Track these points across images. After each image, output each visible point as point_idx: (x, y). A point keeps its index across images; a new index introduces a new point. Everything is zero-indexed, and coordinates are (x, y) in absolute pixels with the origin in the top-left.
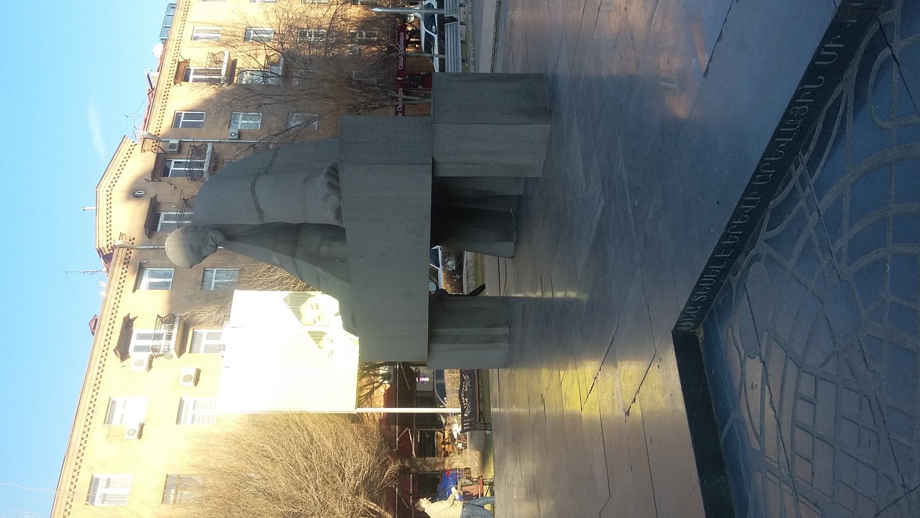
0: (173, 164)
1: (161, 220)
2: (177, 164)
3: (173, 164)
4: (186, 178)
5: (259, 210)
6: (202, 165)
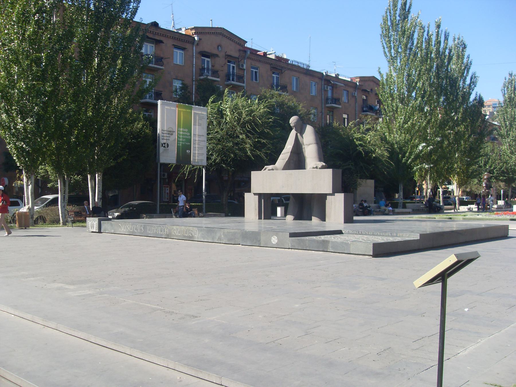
0: (234, 65)
1: (206, 59)
2: (233, 67)
3: (234, 65)
4: (226, 72)
5: (309, 145)
6: (233, 80)
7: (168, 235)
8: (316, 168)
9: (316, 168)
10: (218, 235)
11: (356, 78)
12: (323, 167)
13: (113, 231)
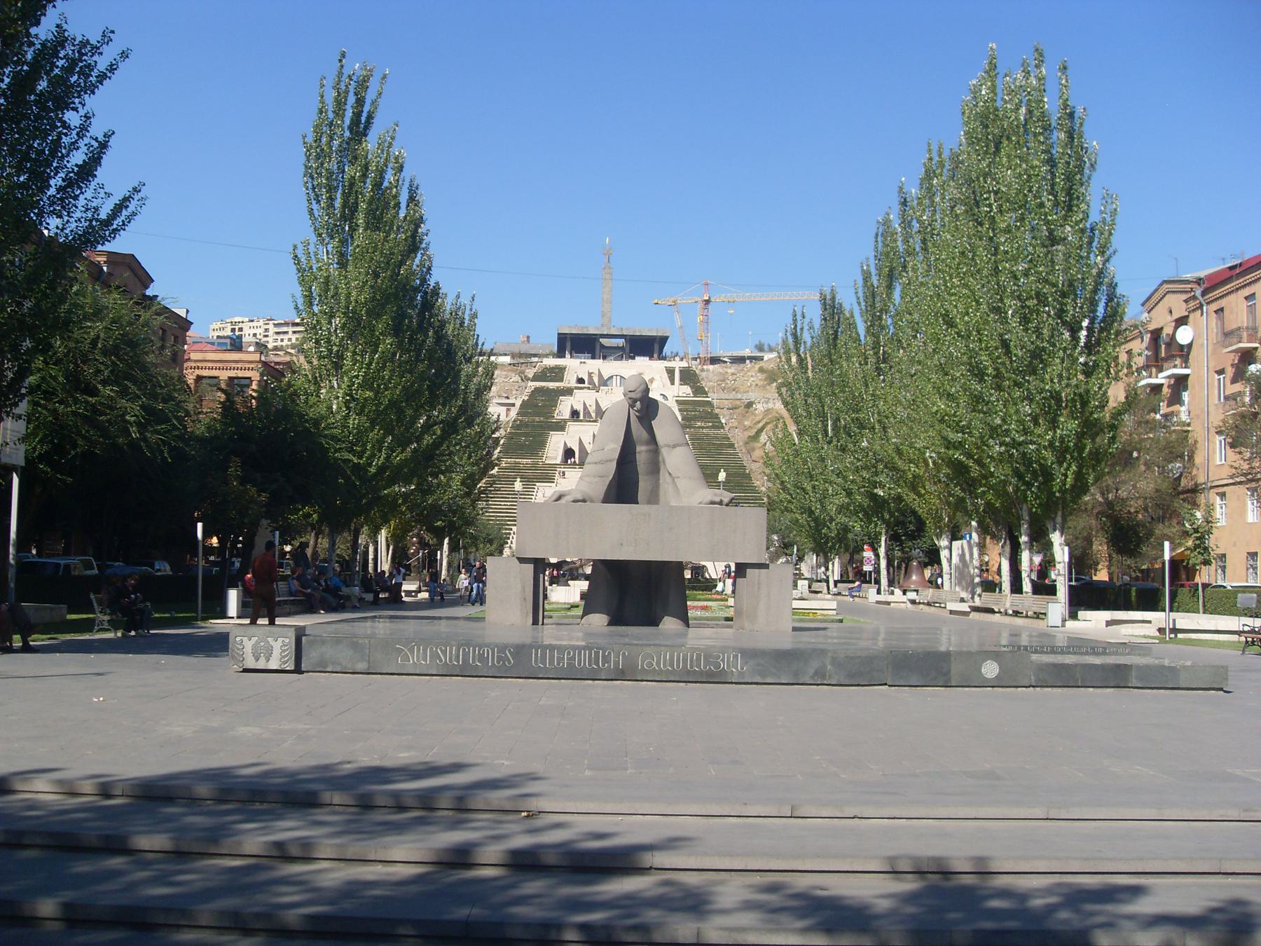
5: (674, 446)
7: (622, 671)
8: (721, 503)
9: (721, 503)
10: (814, 665)
12: (732, 503)
13: (361, 666)
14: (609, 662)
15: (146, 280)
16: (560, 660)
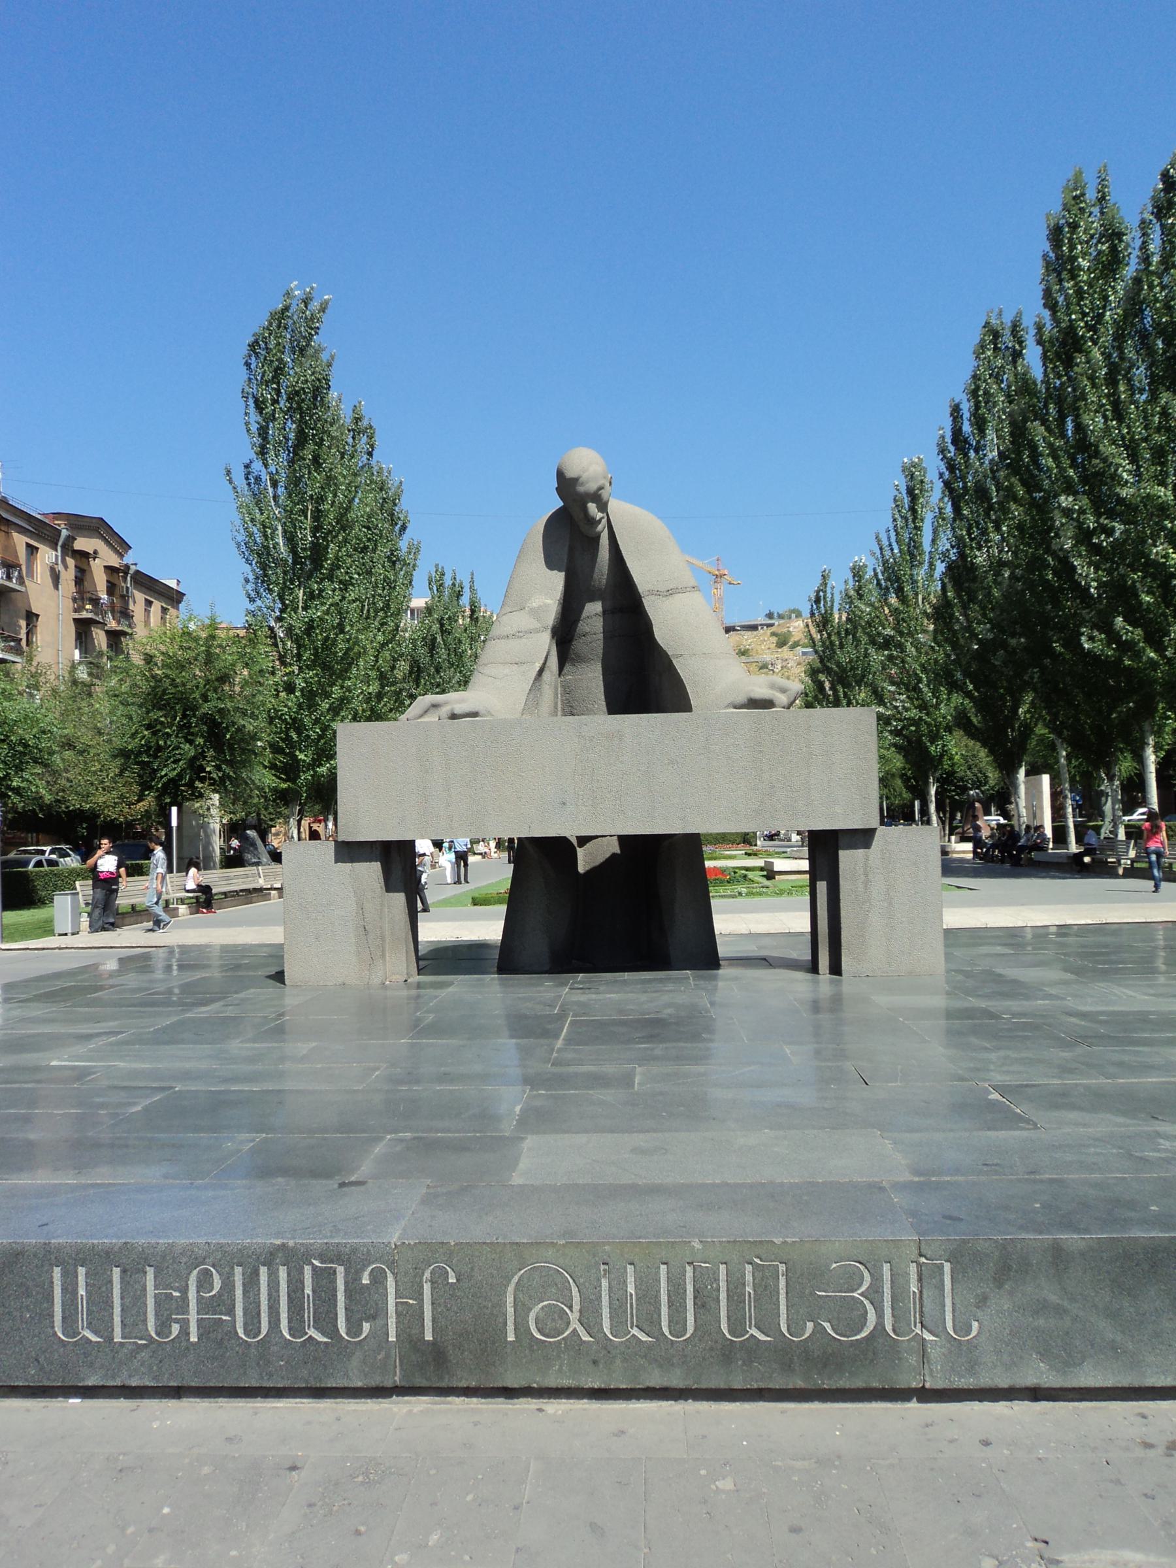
5: (670, 593)
7: (437, 1355)
11: (58, 515)
14: (377, 1314)
15: (120, 545)
16: (170, 1309)
